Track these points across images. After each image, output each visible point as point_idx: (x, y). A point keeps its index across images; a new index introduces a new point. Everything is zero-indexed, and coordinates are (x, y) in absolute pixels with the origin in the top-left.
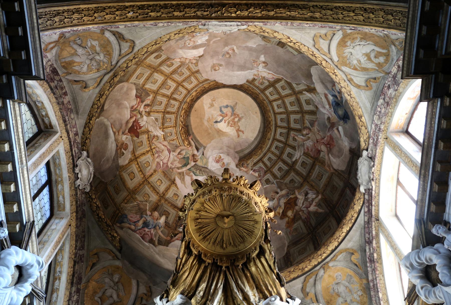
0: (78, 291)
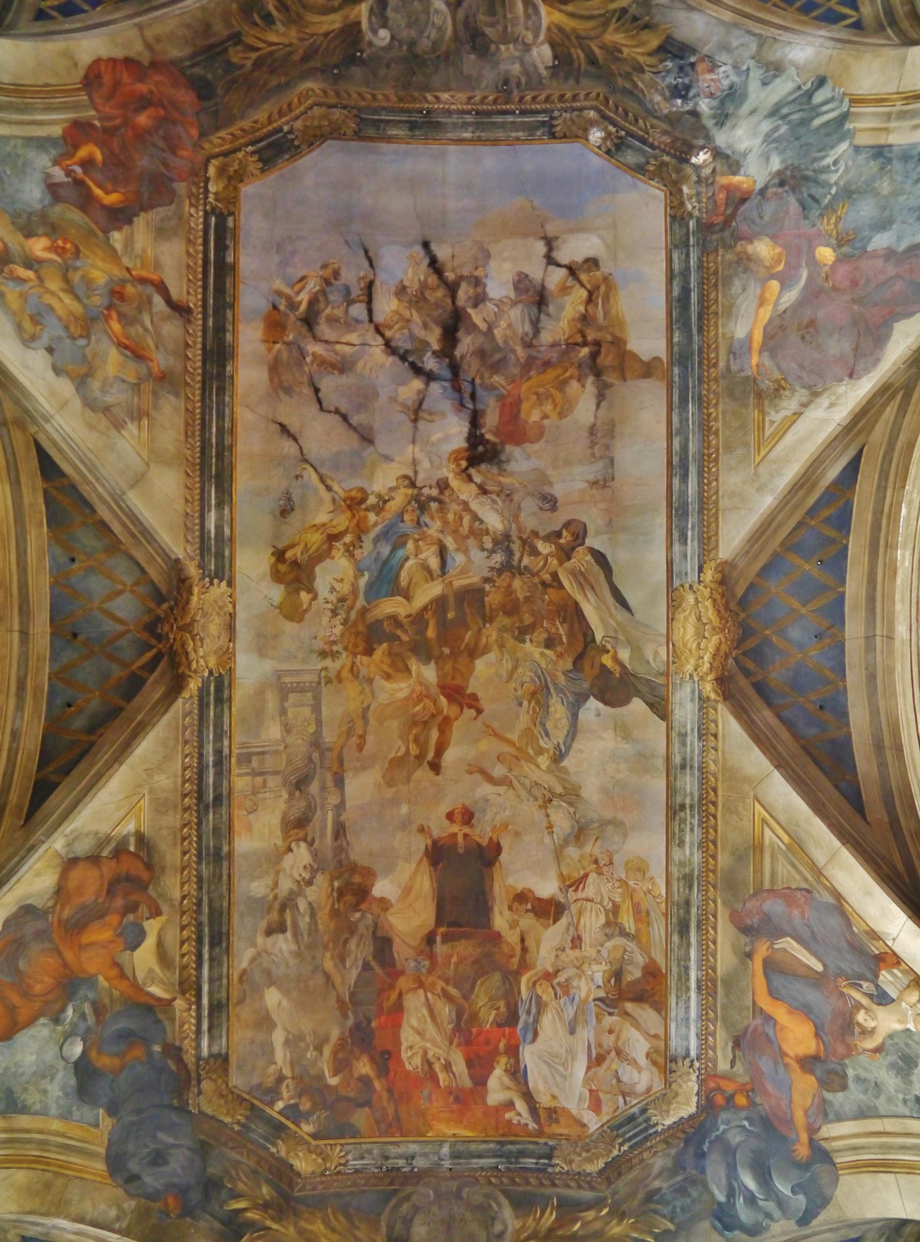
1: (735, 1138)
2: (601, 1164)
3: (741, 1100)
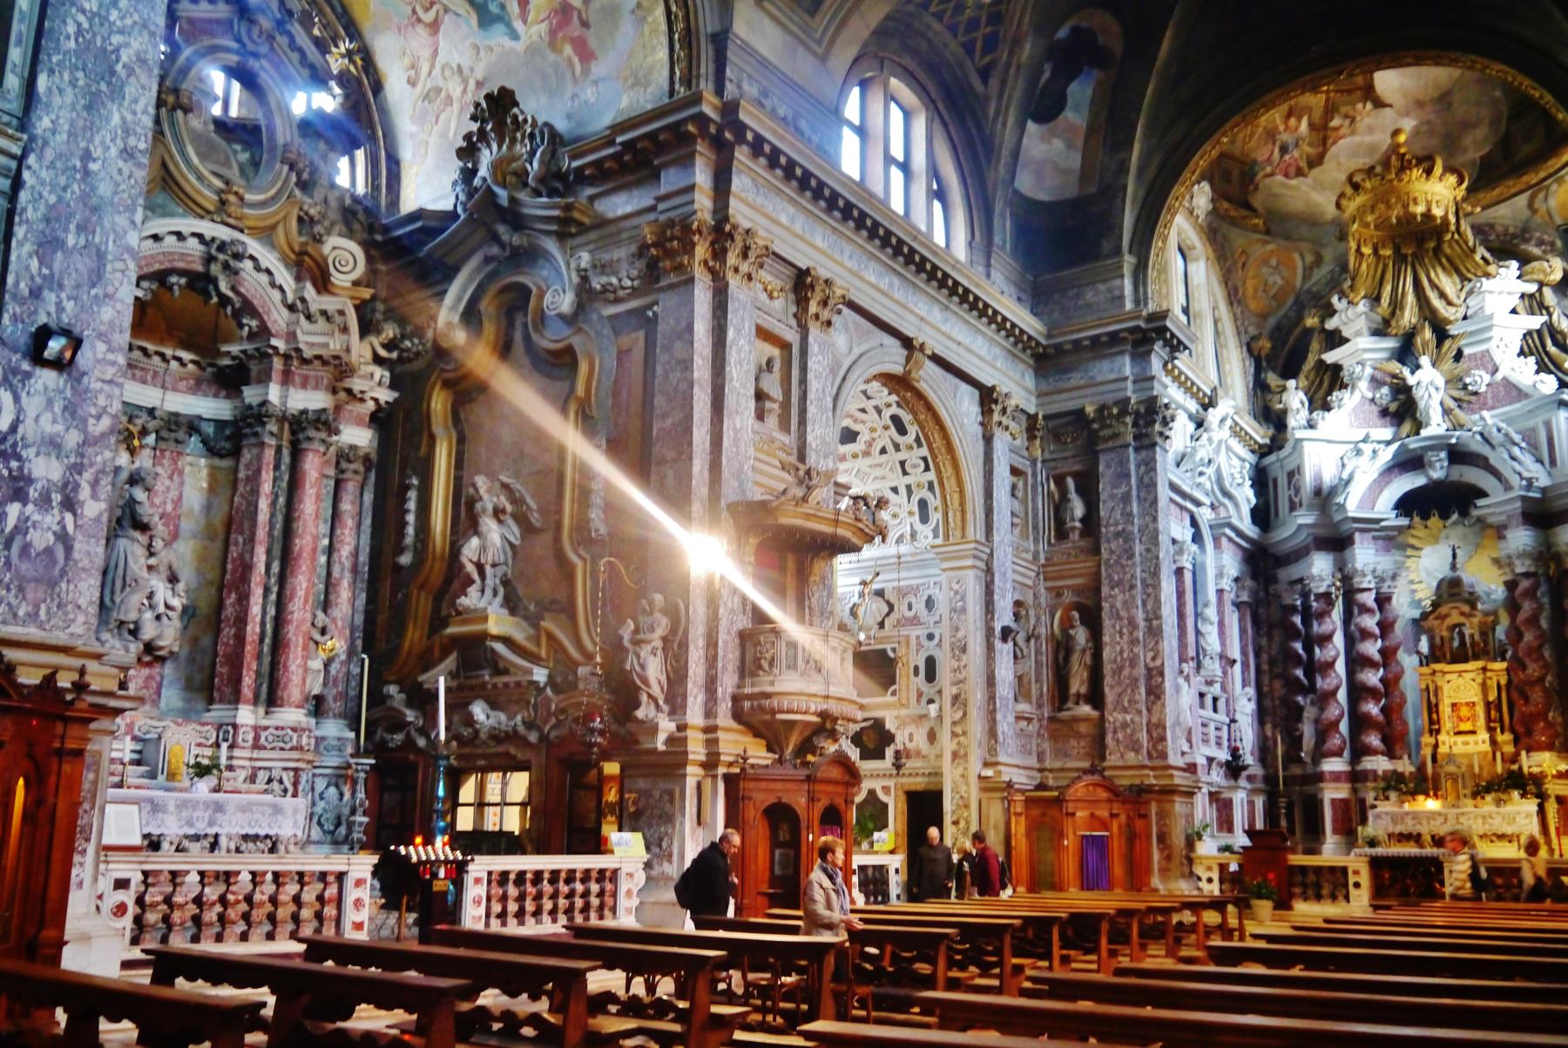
0: (1239, 302)
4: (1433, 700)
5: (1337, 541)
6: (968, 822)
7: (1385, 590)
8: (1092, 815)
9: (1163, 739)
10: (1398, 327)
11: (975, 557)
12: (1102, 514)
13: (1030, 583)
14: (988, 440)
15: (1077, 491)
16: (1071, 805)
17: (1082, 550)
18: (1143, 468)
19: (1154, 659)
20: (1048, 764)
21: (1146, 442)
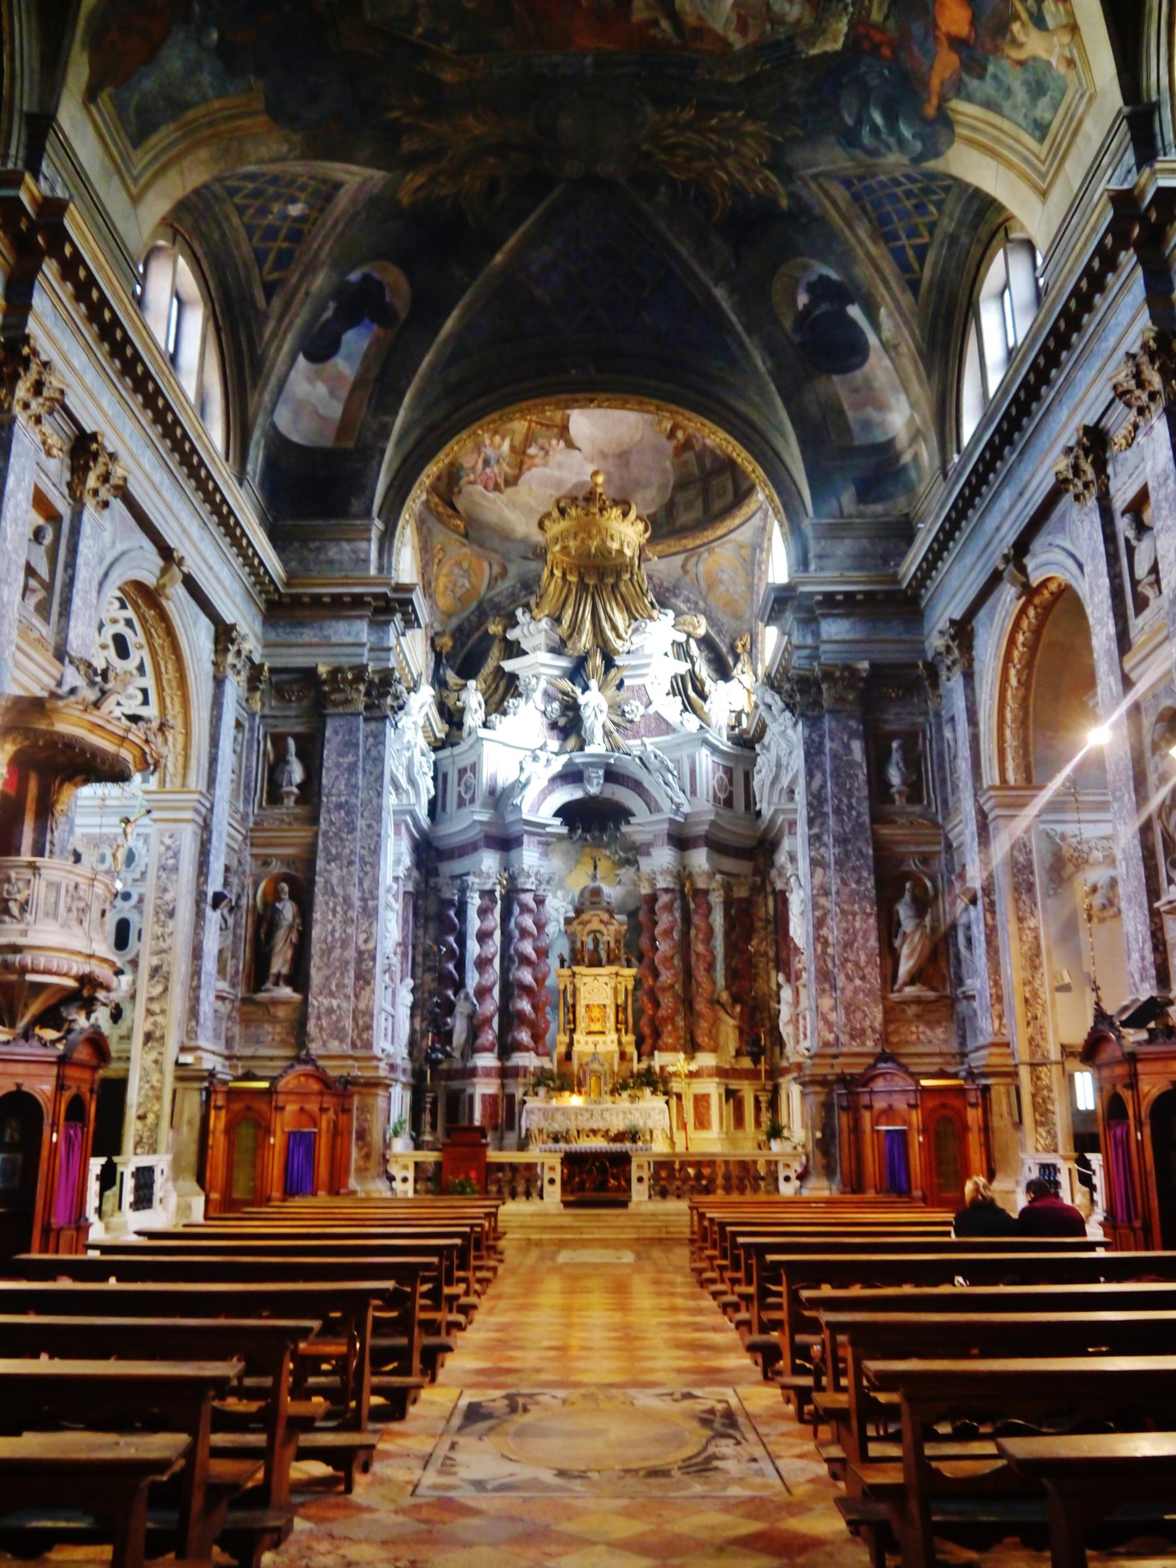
1: (873, 81)
2: (742, 76)
3: (886, 52)
4: (570, 1000)
5: (505, 843)
6: (158, 1117)
7: (540, 892)
8: (302, 1109)
9: (368, 1027)
10: (574, 648)
11: (196, 811)
12: (324, 781)
13: (236, 846)
14: (219, 682)
15: (298, 755)
16: (281, 1098)
17: (297, 818)
18: (371, 740)
19: (366, 941)
20: (238, 1050)
21: (377, 713)
